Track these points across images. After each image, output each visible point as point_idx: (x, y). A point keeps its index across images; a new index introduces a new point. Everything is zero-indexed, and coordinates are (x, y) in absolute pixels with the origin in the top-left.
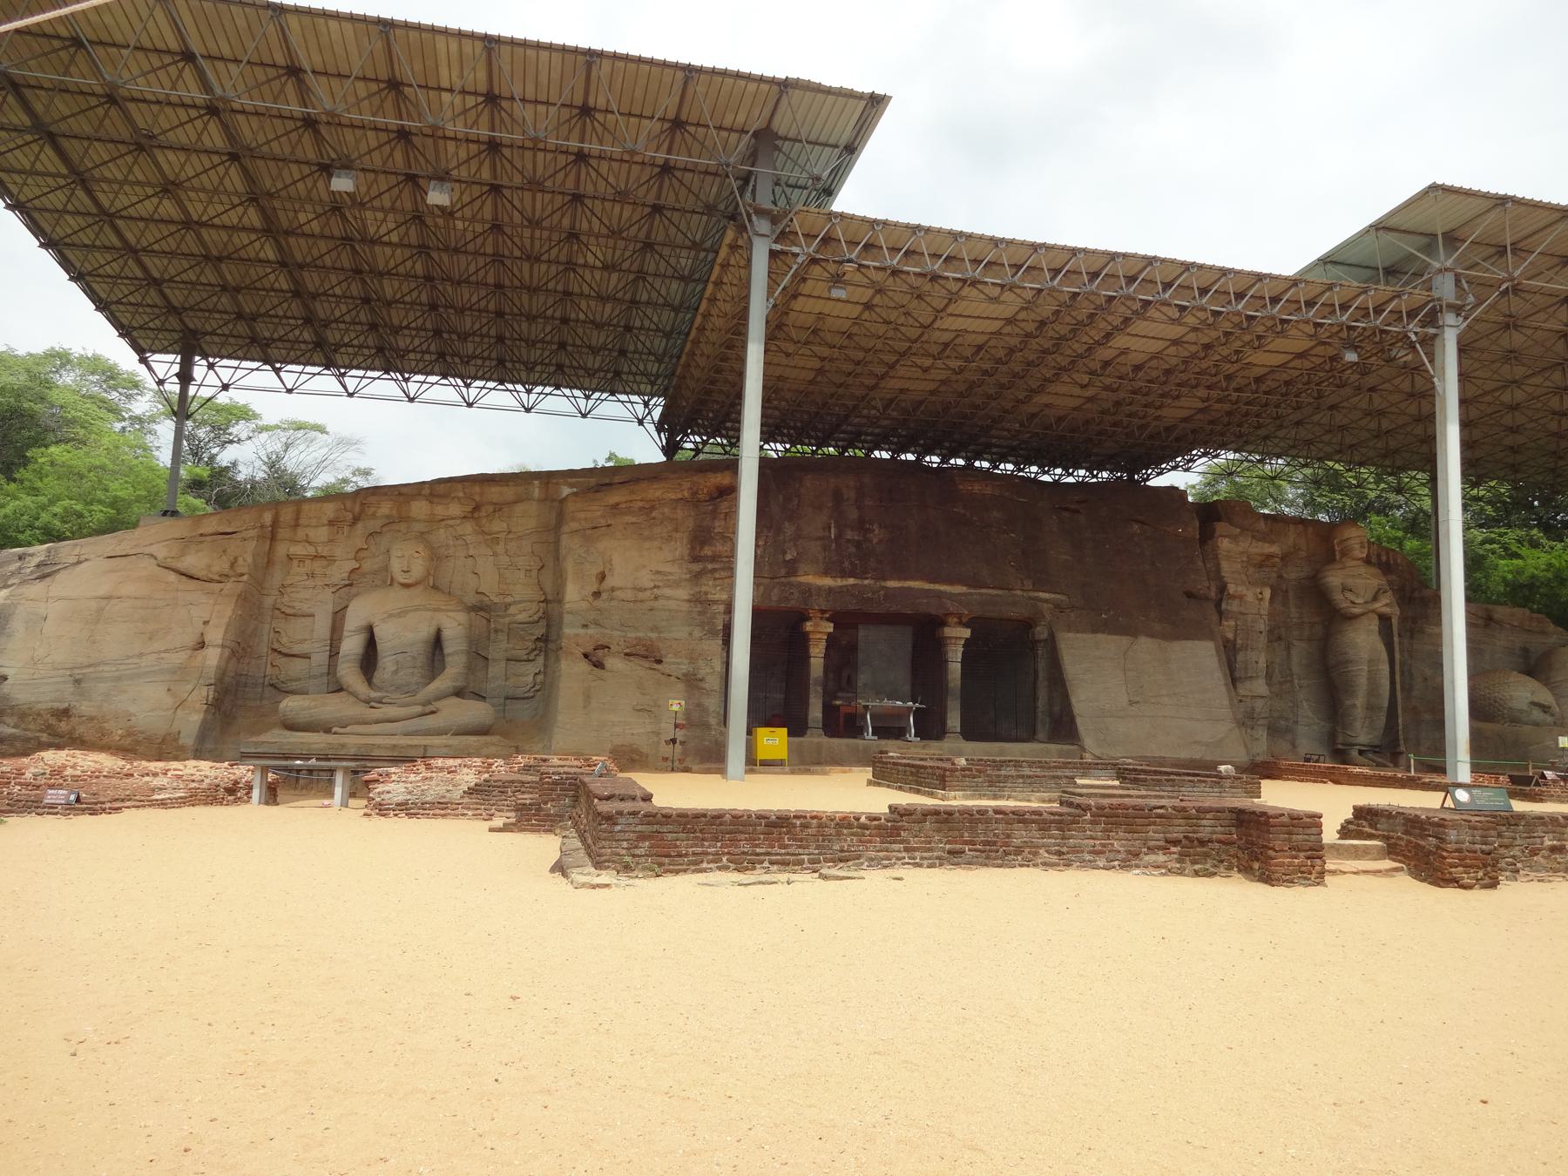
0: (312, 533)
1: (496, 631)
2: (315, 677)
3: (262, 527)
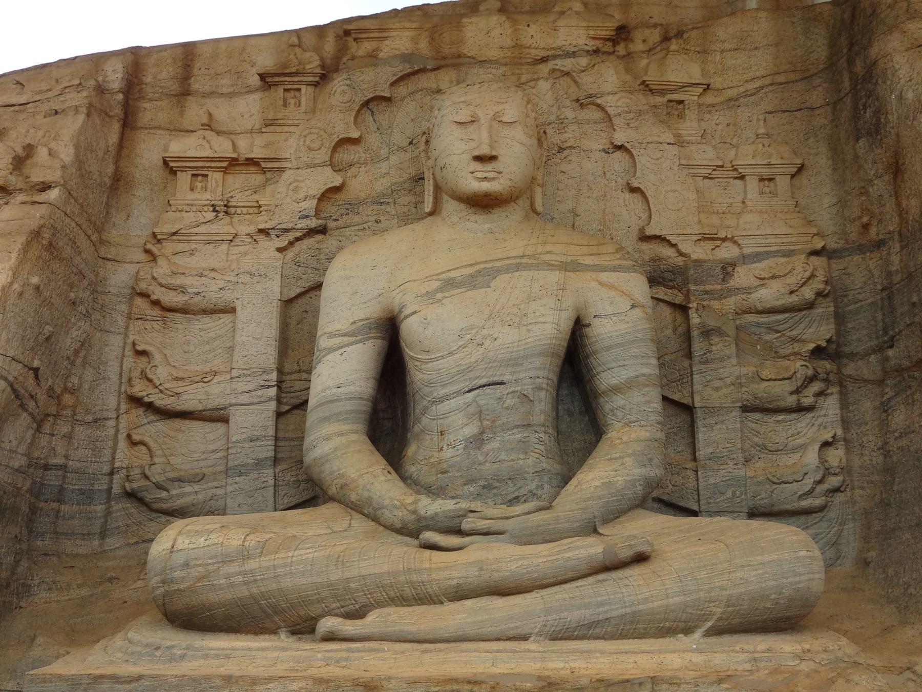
0: (222, 111)
1: (707, 333)
2: (241, 471)
3: (101, 90)
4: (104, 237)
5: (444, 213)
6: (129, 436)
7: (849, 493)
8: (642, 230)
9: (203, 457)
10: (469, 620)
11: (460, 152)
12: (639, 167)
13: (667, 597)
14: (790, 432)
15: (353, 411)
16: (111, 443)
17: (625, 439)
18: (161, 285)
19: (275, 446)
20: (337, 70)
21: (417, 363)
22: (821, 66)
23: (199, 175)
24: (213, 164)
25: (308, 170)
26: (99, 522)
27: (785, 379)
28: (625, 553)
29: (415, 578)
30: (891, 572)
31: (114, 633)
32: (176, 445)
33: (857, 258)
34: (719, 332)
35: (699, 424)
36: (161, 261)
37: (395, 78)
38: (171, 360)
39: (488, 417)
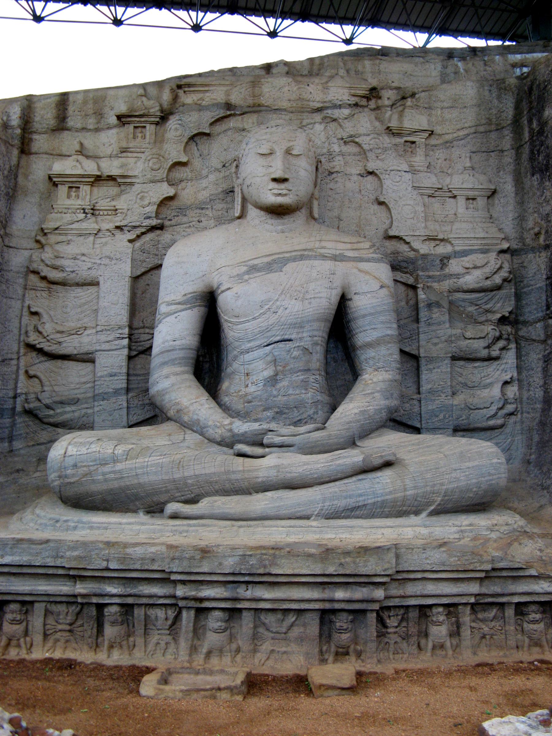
0: (89, 141)
1: (429, 306)
2: (104, 397)
4: (7, 231)
5: (249, 217)
6: (27, 372)
7: (519, 416)
8: (386, 230)
9: (77, 386)
10: (270, 506)
11: (262, 175)
12: (385, 187)
13: (405, 490)
14: (483, 375)
15: (183, 358)
16: (14, 376)
17: (375, 380)
18: (47, 266)
19: (128, 380)
20: (171, 113)
21: (230, 325)
22: (509, 122)
23: (74, 187)
24: (83, 180)
25: (151, 184)
26: (7, 431)
27: (480, 338)
28: (378, 462)
29: (233, 477)
30: (545, 469)
31: (24, 509)
32: (59, 378)
33: (531, 256)
34: (438, 305)
35: (423, 368)
36: (47, 249)
37: (213, 120)
38: (54, 318)
39: (280, 364)
